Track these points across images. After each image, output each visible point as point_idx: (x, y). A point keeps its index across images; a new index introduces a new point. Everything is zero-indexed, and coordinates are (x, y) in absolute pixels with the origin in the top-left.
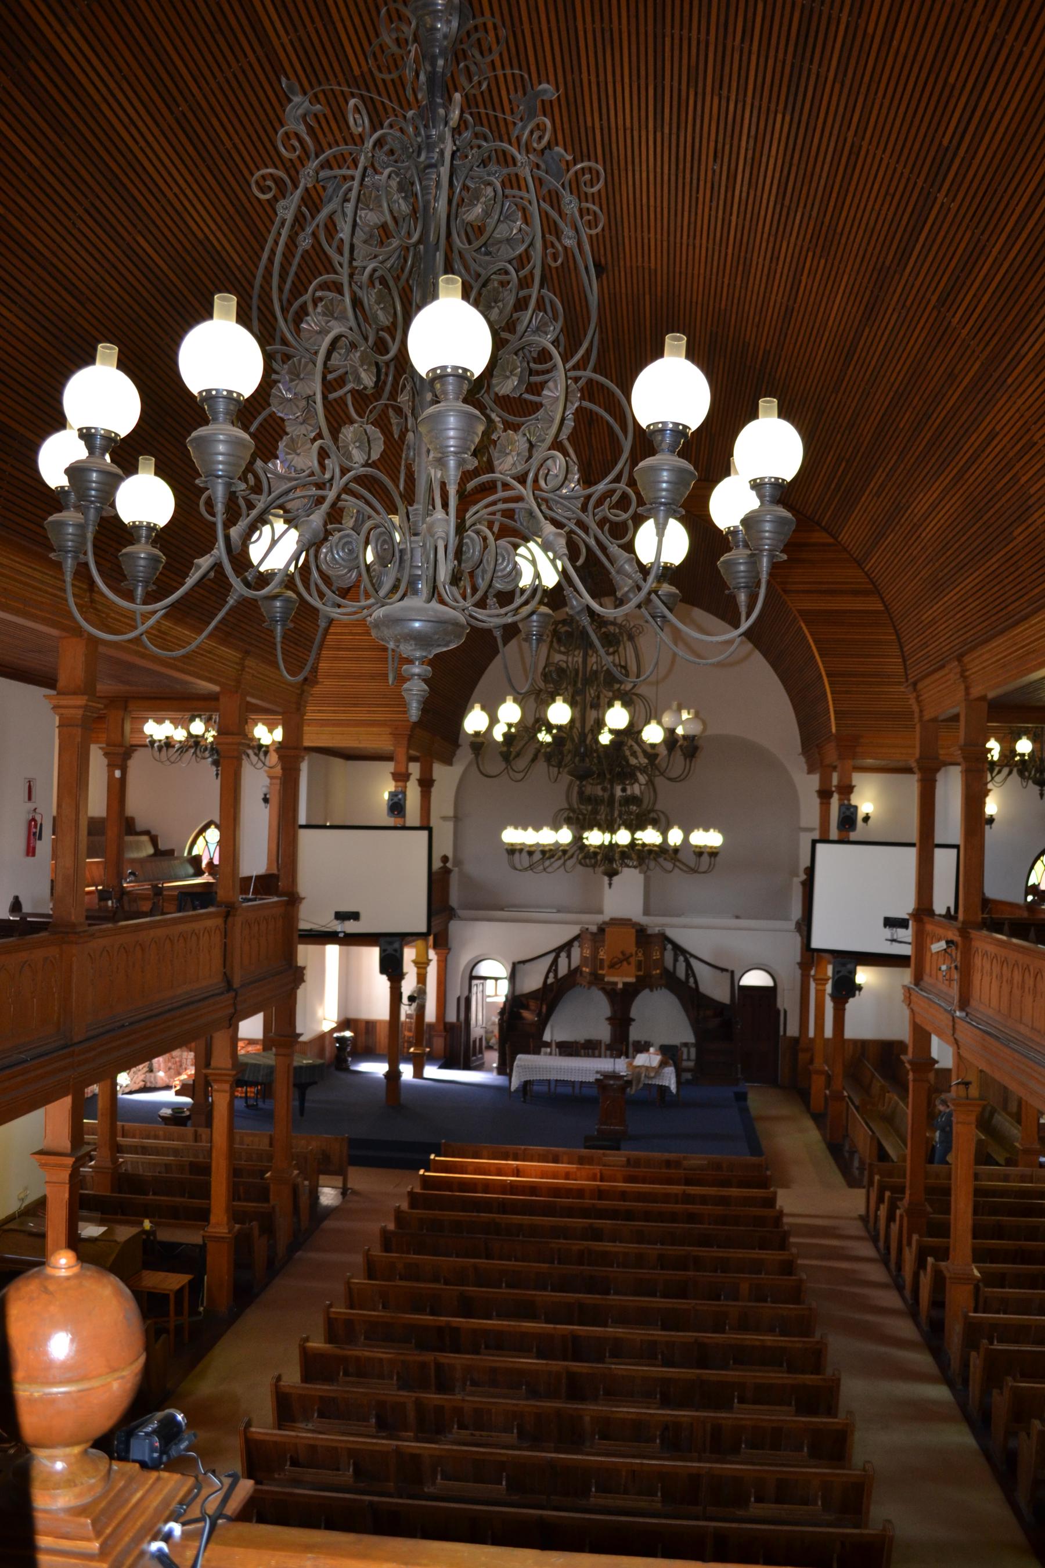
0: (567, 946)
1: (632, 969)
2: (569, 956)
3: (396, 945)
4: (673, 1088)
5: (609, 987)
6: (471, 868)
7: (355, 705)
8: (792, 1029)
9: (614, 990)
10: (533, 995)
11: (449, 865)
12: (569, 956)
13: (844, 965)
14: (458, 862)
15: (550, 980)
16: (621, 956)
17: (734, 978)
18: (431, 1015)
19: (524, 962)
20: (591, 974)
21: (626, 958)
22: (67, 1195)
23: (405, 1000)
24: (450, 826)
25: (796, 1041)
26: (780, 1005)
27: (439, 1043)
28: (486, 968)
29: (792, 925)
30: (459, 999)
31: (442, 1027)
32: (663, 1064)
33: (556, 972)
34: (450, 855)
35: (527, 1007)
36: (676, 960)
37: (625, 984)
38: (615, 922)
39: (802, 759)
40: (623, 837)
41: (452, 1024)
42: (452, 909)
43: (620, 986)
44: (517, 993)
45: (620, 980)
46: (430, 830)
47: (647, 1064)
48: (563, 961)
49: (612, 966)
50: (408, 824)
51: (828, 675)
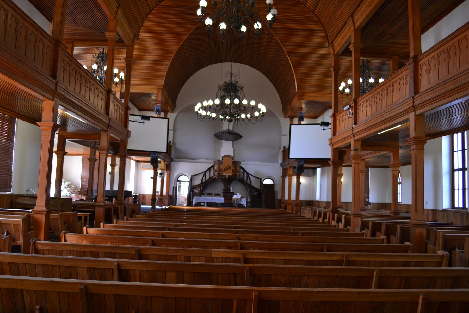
0: (209, 169)
1: (231, 171)
2: (210, 172)
3: (156, 155)
5: (223, 178)
6: (178, 146)
7: (145, 79)
8: (279, 197)
9: (225, 178)
11: (171, 144)
12: (210, 172)
13: (300, 162)
14: (174, 144)
15: (204, 180)
17: (261, 182)
18: (165, 193)
19: (195, 175)
21: (229, 168)
22: (50, 139)
23: (159, 175)
25: (280, 200)
26: (275, 190)
27: (167, 201)
28: (181, 179)
30: (173, 187)
32: (242, 197)
33: (205, 178)
34: (172, 141)
35: (196, 189)
36: (244, 173)
39: (283, 114)
40: (236, 101)
42: (172, 159)
43: (227, 176)
44: (193, 185)
45: (228, 174)
46: (168, 119)
48: (208, 174)
49: (225, 170)
51: (295, 73)
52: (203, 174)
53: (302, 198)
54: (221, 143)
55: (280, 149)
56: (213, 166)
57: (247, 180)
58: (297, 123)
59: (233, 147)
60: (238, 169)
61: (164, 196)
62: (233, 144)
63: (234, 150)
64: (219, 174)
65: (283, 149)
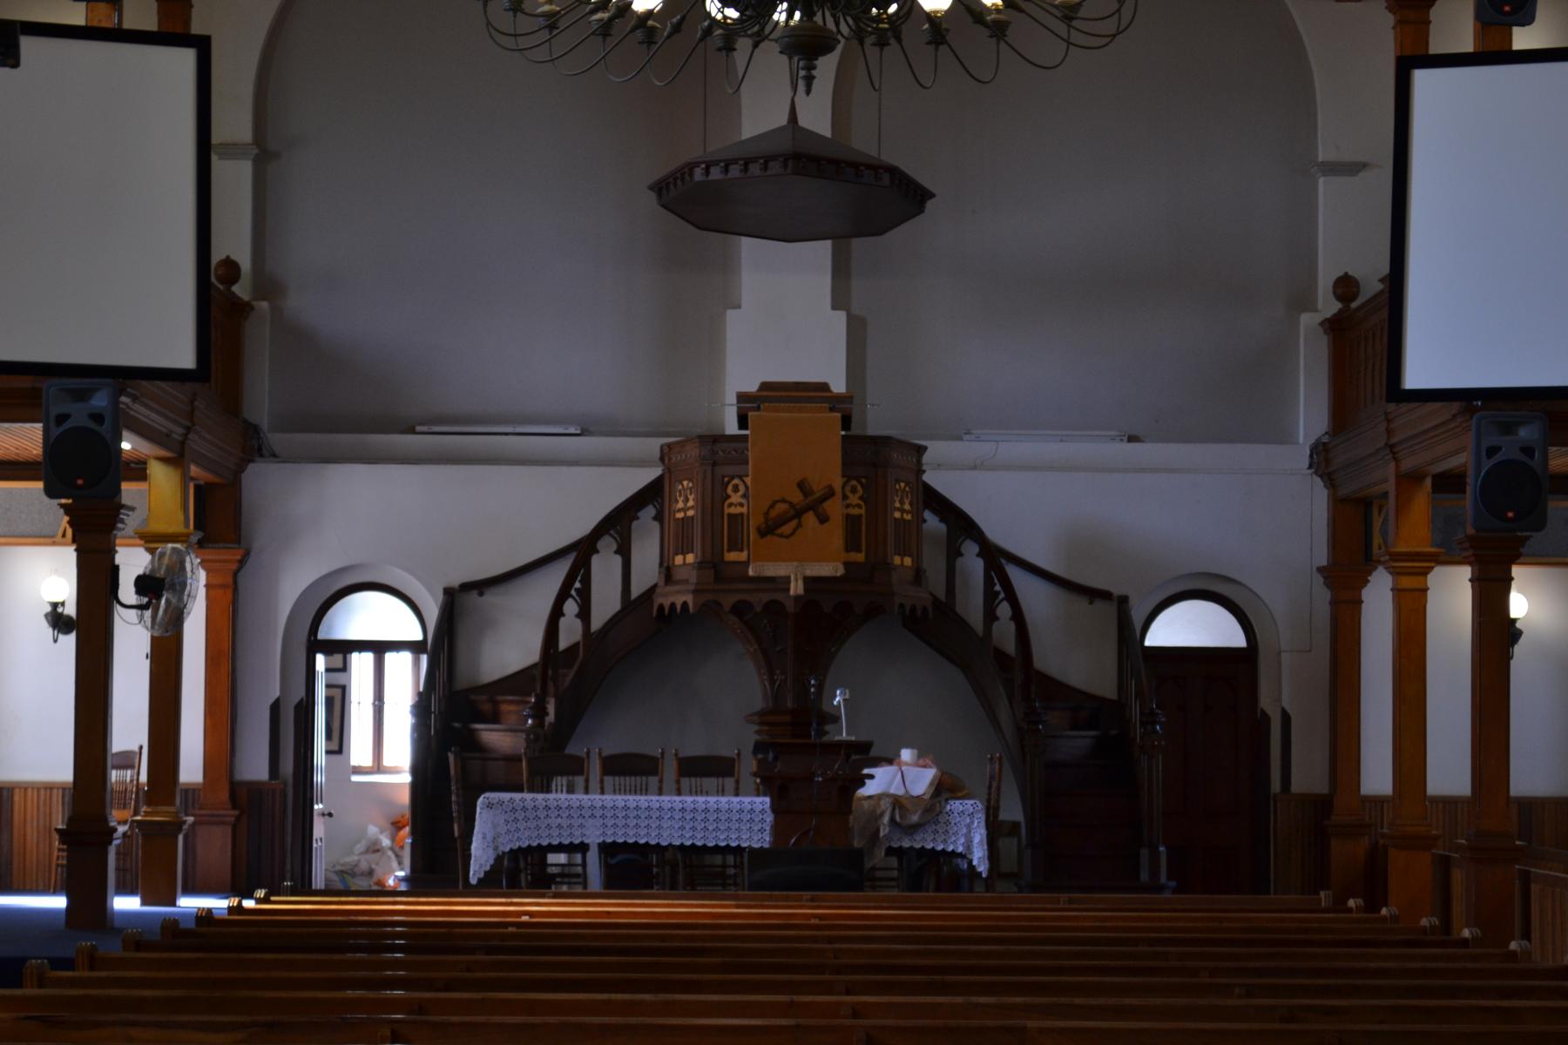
0: (618, 523)
1: (834, 535)
2: (624, 551)
3: (100, 401)
4: (979, 858)
5: (759, 599)
6: (306, 305)
8: (1308, 773)
9: (774, 608)
10: (516, 683)
11: (241, 290)
12: (624, 551)
13: (1508, 428)
14: (268, 287)
16: (797, 497)
17: (1129, 633)
19: (481, 586)
20: (701, 565)
21: (813, 503)
23: (127, 592)
24: (245, 168)
25: (1321, 805)
26: (1265, 702)
27: (216, 846)
29: (1299, 456)
30: (275, 708)
31: (225, 795)
32: (945, 789)
33: (584, 614)
34: (245, 262)
35: (494, 718)
36: (954, 553)
37: (808, 581)
38: (773, 394)
41: (254, 788)
42: (252, 431)
43: (796, 588)
45: (799, 566)
46: (202, 46)
47: (896, 789)
48: (606, 567)
49: (767, 530)
50: (128, 24)
52: (560, 571)
53: (1532, 773)
54: (728, 266)
55: (1303, 301)
56: (651, 494)
57: (990, 616)
58: (1467, 46)
59: (840, 300)
60: (901, 508)
61: (191, 791)
62: (841, 270)
63: (857, 334)
64: (712, 566)
65: (1329, 306)
